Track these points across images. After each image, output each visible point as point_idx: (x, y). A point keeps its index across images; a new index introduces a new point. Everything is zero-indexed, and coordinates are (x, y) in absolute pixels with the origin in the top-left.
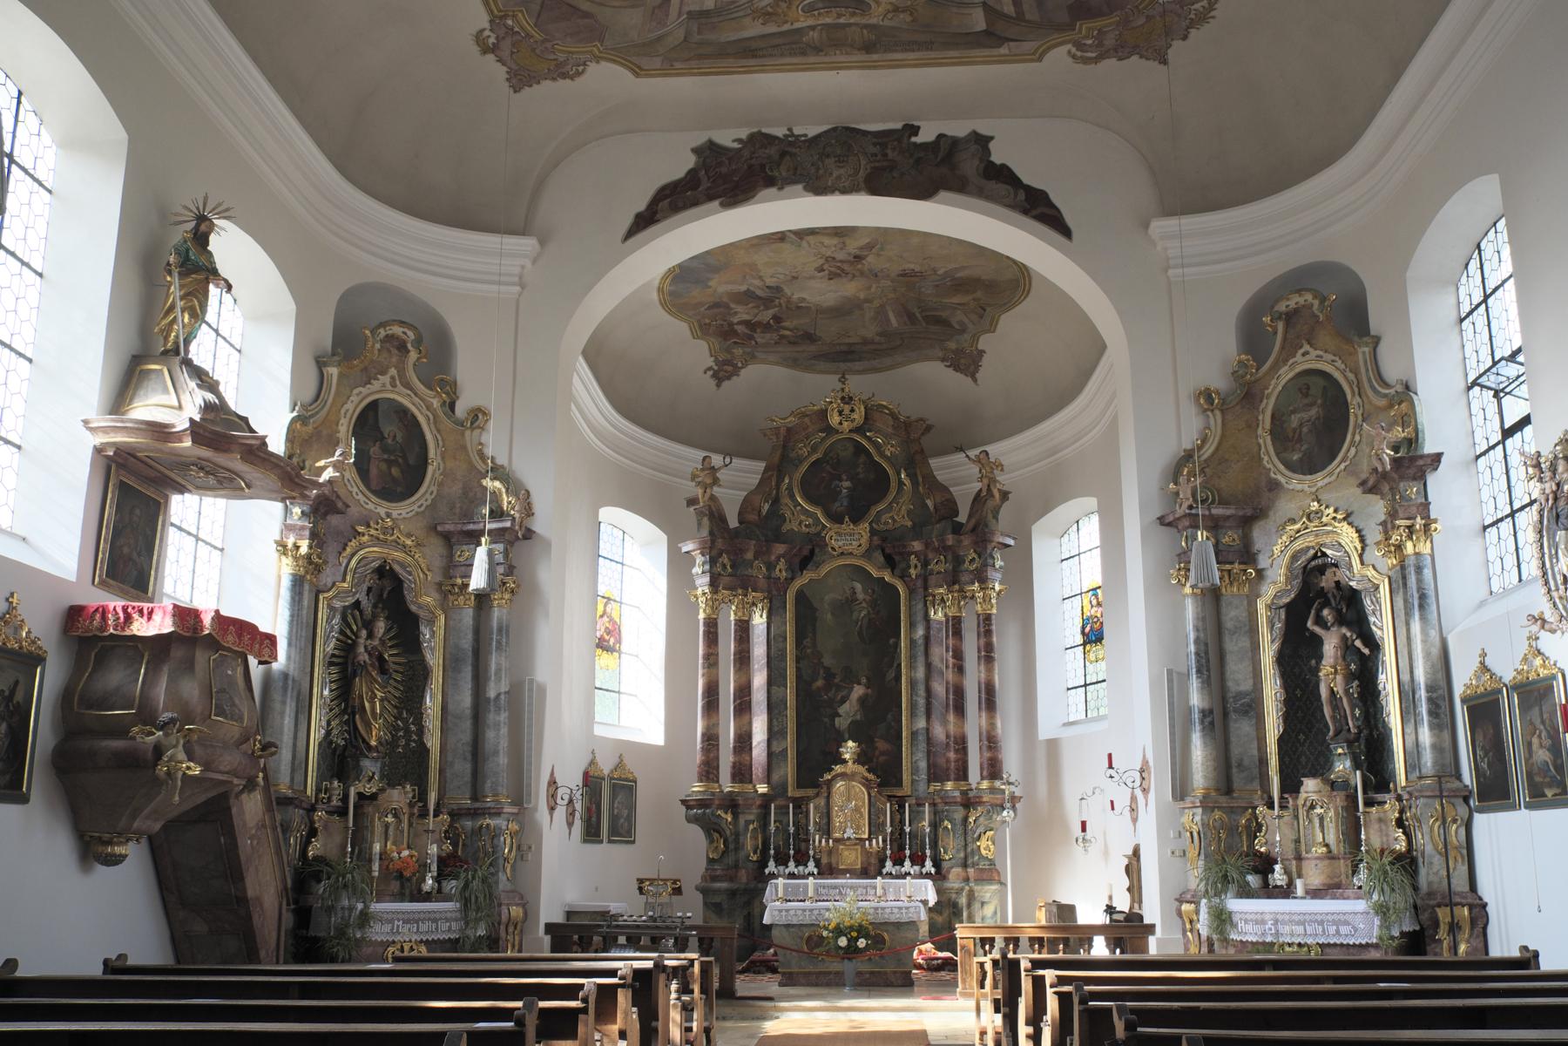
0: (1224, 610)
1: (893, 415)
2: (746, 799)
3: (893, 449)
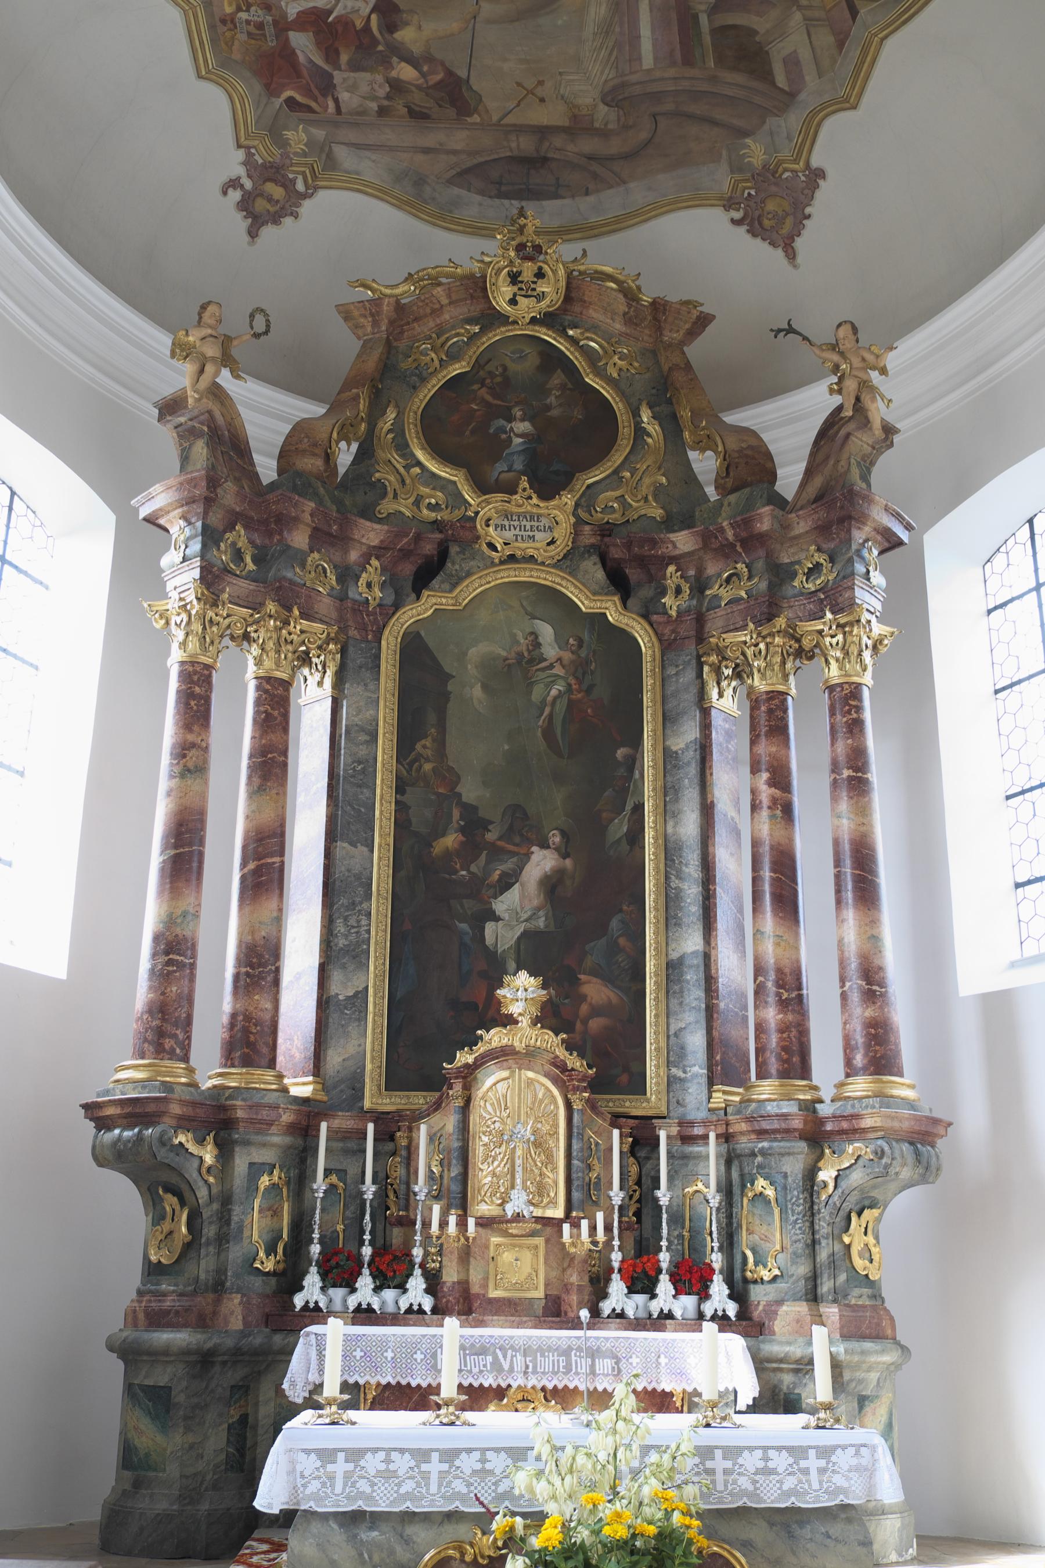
1: (630, 295)
3: (619, 362)
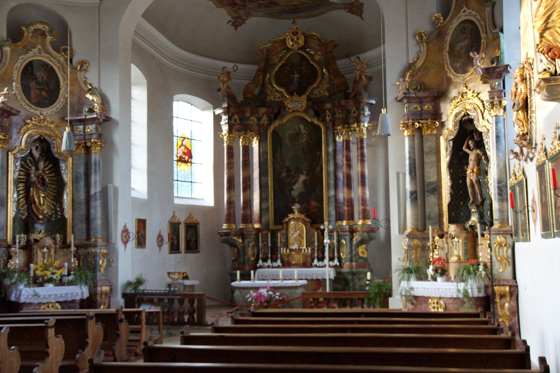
0: (424, 143)
2: (248, 231)
3: (319, 57)
